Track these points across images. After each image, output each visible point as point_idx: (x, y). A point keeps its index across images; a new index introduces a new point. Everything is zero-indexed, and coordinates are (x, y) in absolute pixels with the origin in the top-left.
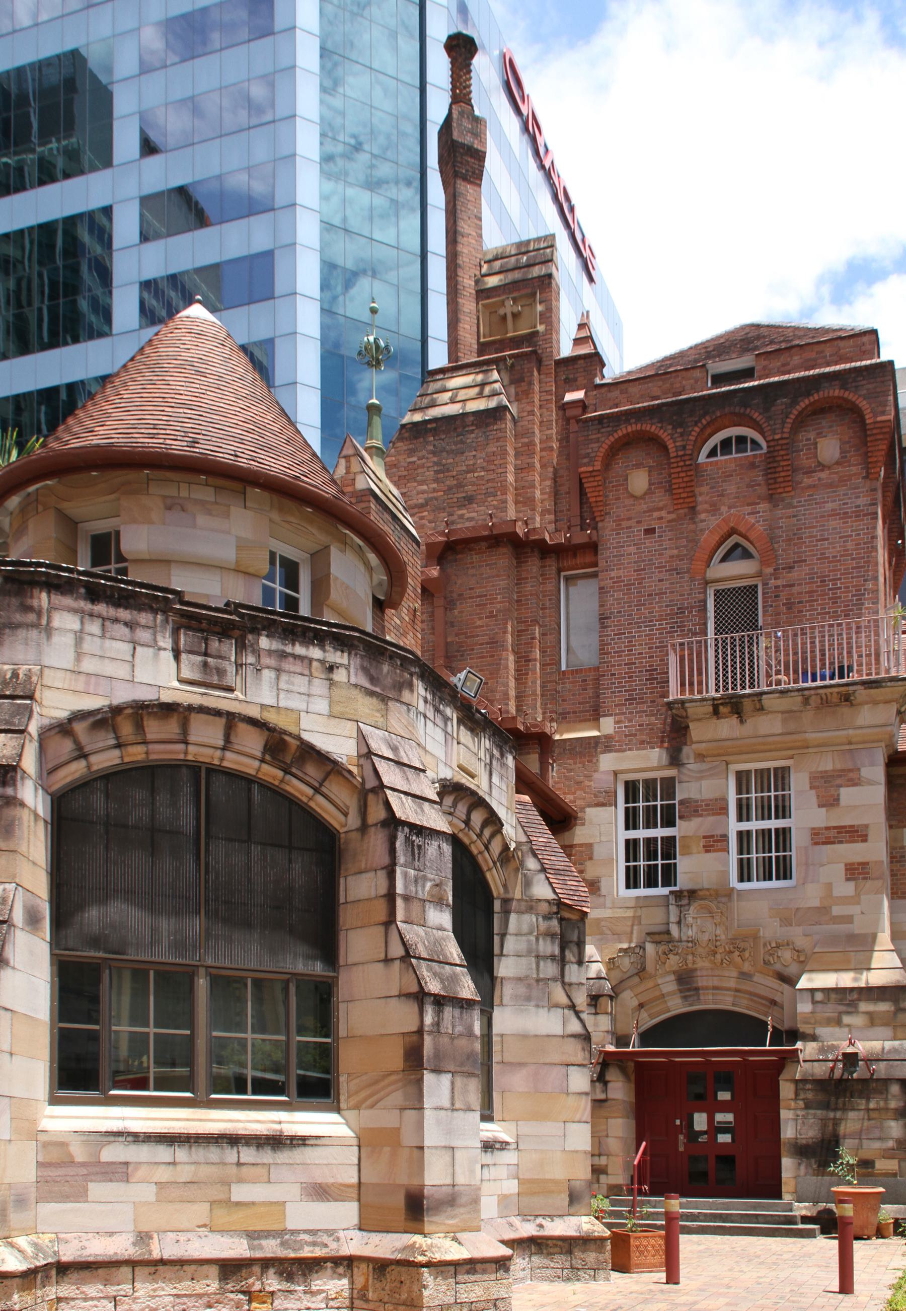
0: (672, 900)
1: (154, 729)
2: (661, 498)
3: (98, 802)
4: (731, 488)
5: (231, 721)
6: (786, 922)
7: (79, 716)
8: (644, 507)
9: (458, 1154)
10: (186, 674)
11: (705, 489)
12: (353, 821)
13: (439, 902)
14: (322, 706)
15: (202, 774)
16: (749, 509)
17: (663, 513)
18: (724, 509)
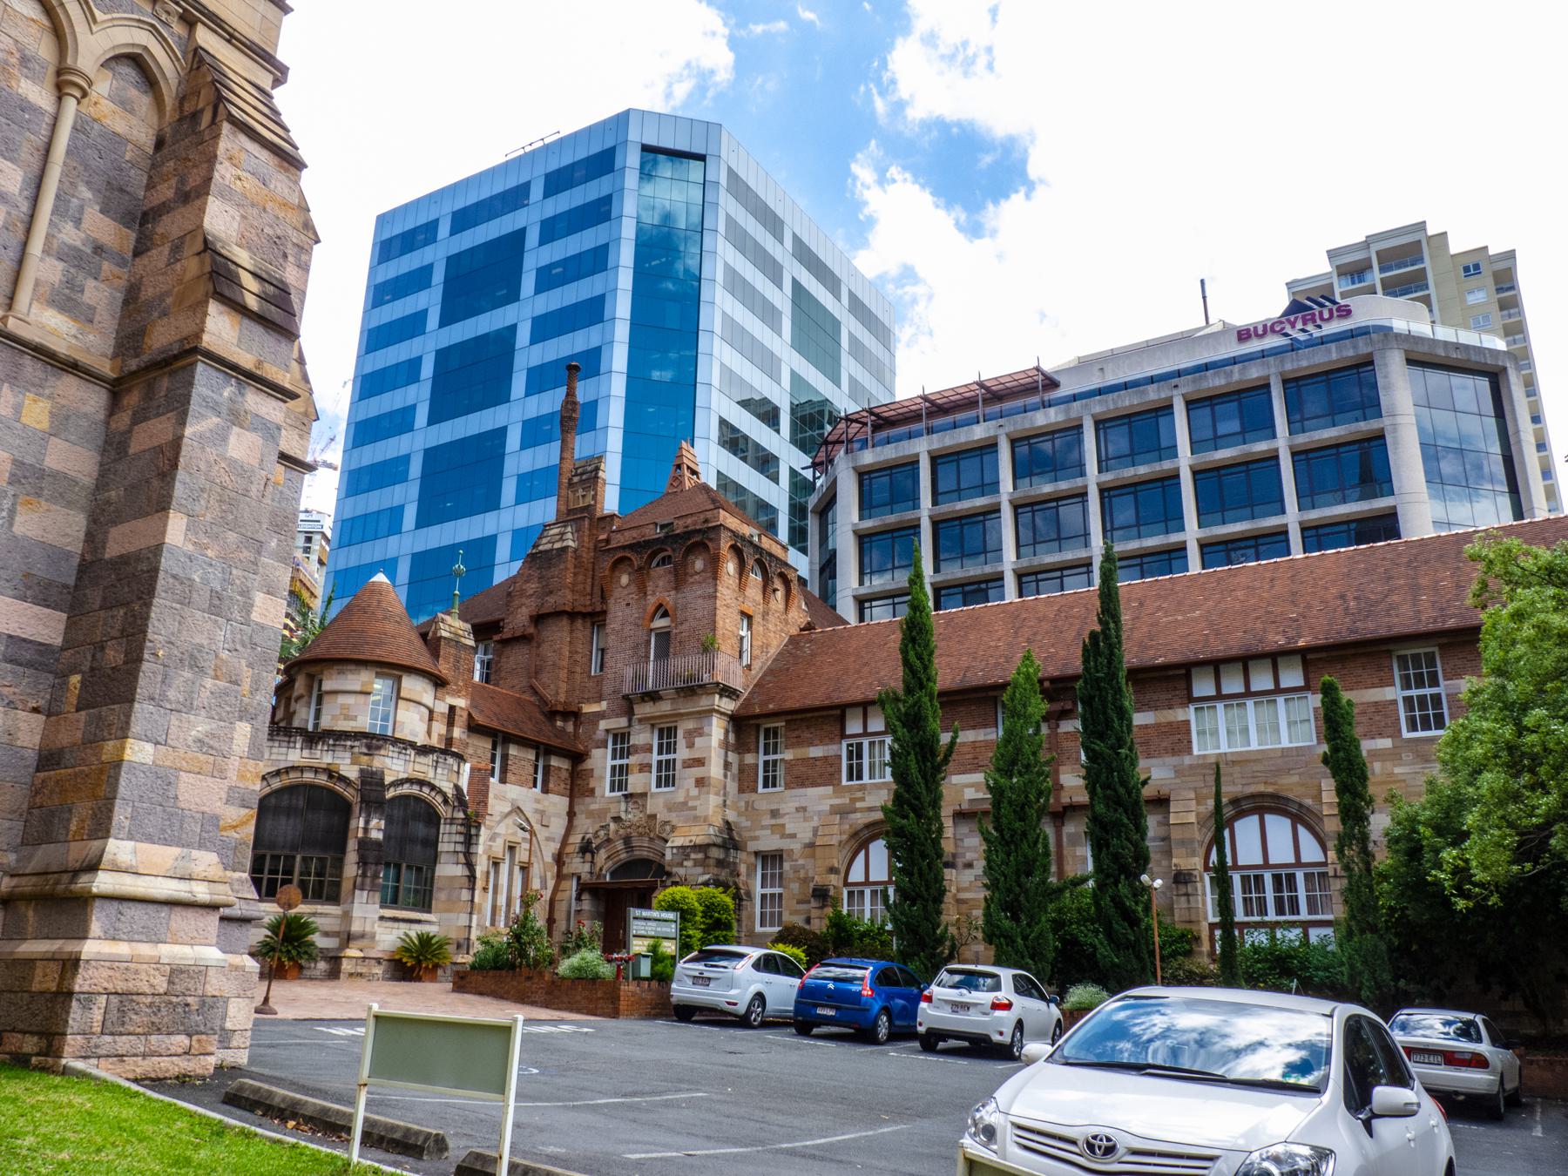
2: (633, 588)
3: (273, 801)
4: (661, 583)
6: (670, 810)
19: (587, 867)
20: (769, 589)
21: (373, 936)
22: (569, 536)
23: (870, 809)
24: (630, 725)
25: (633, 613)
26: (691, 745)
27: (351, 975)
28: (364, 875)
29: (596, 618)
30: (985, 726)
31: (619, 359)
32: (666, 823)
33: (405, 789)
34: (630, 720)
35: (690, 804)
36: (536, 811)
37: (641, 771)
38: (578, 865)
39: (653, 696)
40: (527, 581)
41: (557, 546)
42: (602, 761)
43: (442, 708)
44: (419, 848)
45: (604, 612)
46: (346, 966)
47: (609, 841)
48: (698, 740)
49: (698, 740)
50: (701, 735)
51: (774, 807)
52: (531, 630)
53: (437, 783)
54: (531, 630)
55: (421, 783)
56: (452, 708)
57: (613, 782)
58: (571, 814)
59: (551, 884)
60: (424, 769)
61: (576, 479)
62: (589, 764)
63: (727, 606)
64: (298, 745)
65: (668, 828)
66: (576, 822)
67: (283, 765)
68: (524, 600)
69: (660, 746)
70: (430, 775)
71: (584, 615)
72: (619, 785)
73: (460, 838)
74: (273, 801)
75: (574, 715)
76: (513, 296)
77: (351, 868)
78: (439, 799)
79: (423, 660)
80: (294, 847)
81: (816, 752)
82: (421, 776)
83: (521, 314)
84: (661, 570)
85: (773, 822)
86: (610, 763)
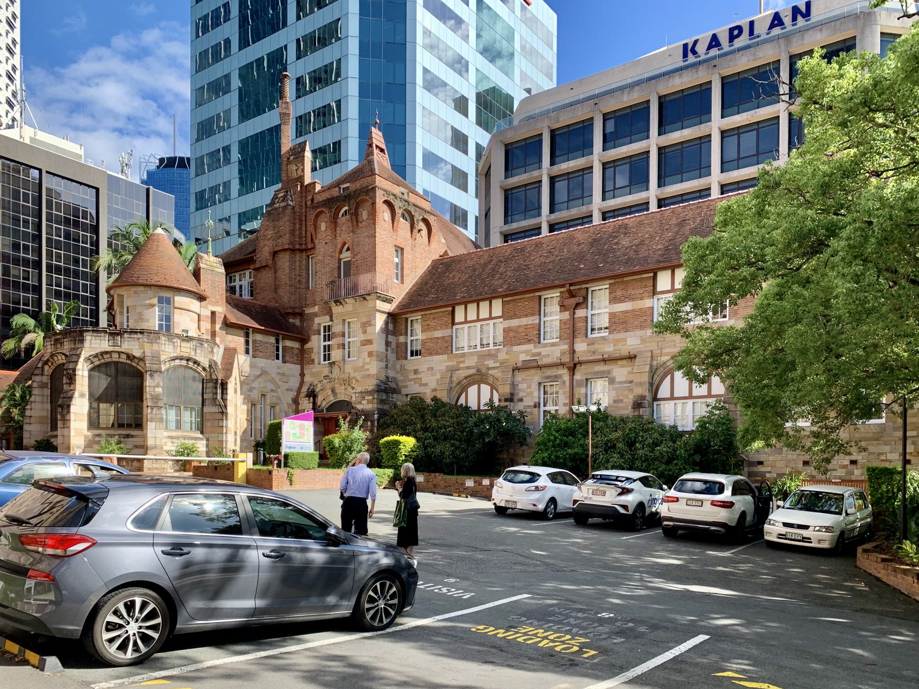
1: (105, 356)
5: (119, 353)
6: (355, 371)
20: (415, 231)
23: (468, 368)
26: (365, 332)
30: (533, 315)
31: (352, 67)
35: (366, 367)
43: (206, 313)
50: (370, 325)
51: (416, 368)
53: (198, 359)
57: (325, 355)
58: (302, 375)
60: (188, 350)
63: (385, 242)
70: (192, 355)
72: (327, 357)
79: (189, 283)
81: (438, 334)
82: (186, 355)
85: (415, 376)
86: (323, 344)
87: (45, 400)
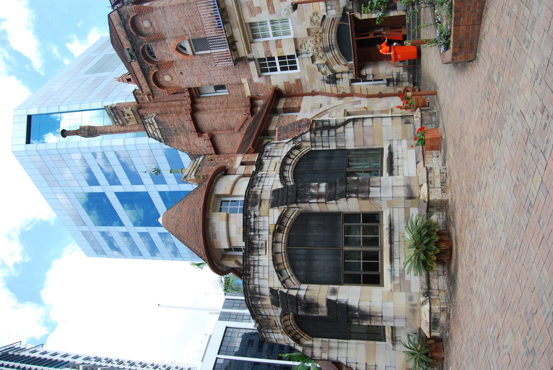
0: (300, 57)
2: (171, 71)
4: (164, 51)
6: (303, 19)
7: (279, 279)
8: (175, 76)
9: (394, 185)
10: (264, 253)
11: (166, 59)
12: (297, 209)
13: (318, 186)
14: (266, 218)
15: (289, 243)
16: (169, 45)
17: (175, 70)
18: (170, 53)
19: (345, 76)
21: (409, 178)
22: (149, 120)
24: (253, 59)
25: (185, 68)
26: (259, 9)
27: (443, 191)
28: (357, 192)
29: (195, 94)
32: (312, 20)
33: (289, 175)
34: (250, 60)
36: (312, 111)
37: (281, 47)
38: (344, 84)
39: (232, 44)
40: (181, 143)
41: (157, 127)
42: (279, 78)
44: (333, 161)
45: (190, 89)
46: (436, 196)
47: (327, 64)
48: (256, 4)
49: (256, 4)
52: (206, 135)
53: (284, 155)
54: (206, 135)
55: (284, 163)
56: (242, 164)
58: (314, 94)
59: (357, 99)
61: (121, 122)
62: (281, 86)
64: (257, 258)
65: (315, 18)
66: (318, 90)
67: (272, 269)
68: (191, 143)
69: (264, 36)
70: (279, 160)
71: (193, 103)
73: (325, 133)
74: (301, 273)
75: (252, 100)
76: (103, 195)
77: (351, 205)
78: (296, 152)
80: (337, 253)
82: (279, 165)
83: (111, 192)
84: (156, 53)
86: (279, 72)
87: (345, 345)
